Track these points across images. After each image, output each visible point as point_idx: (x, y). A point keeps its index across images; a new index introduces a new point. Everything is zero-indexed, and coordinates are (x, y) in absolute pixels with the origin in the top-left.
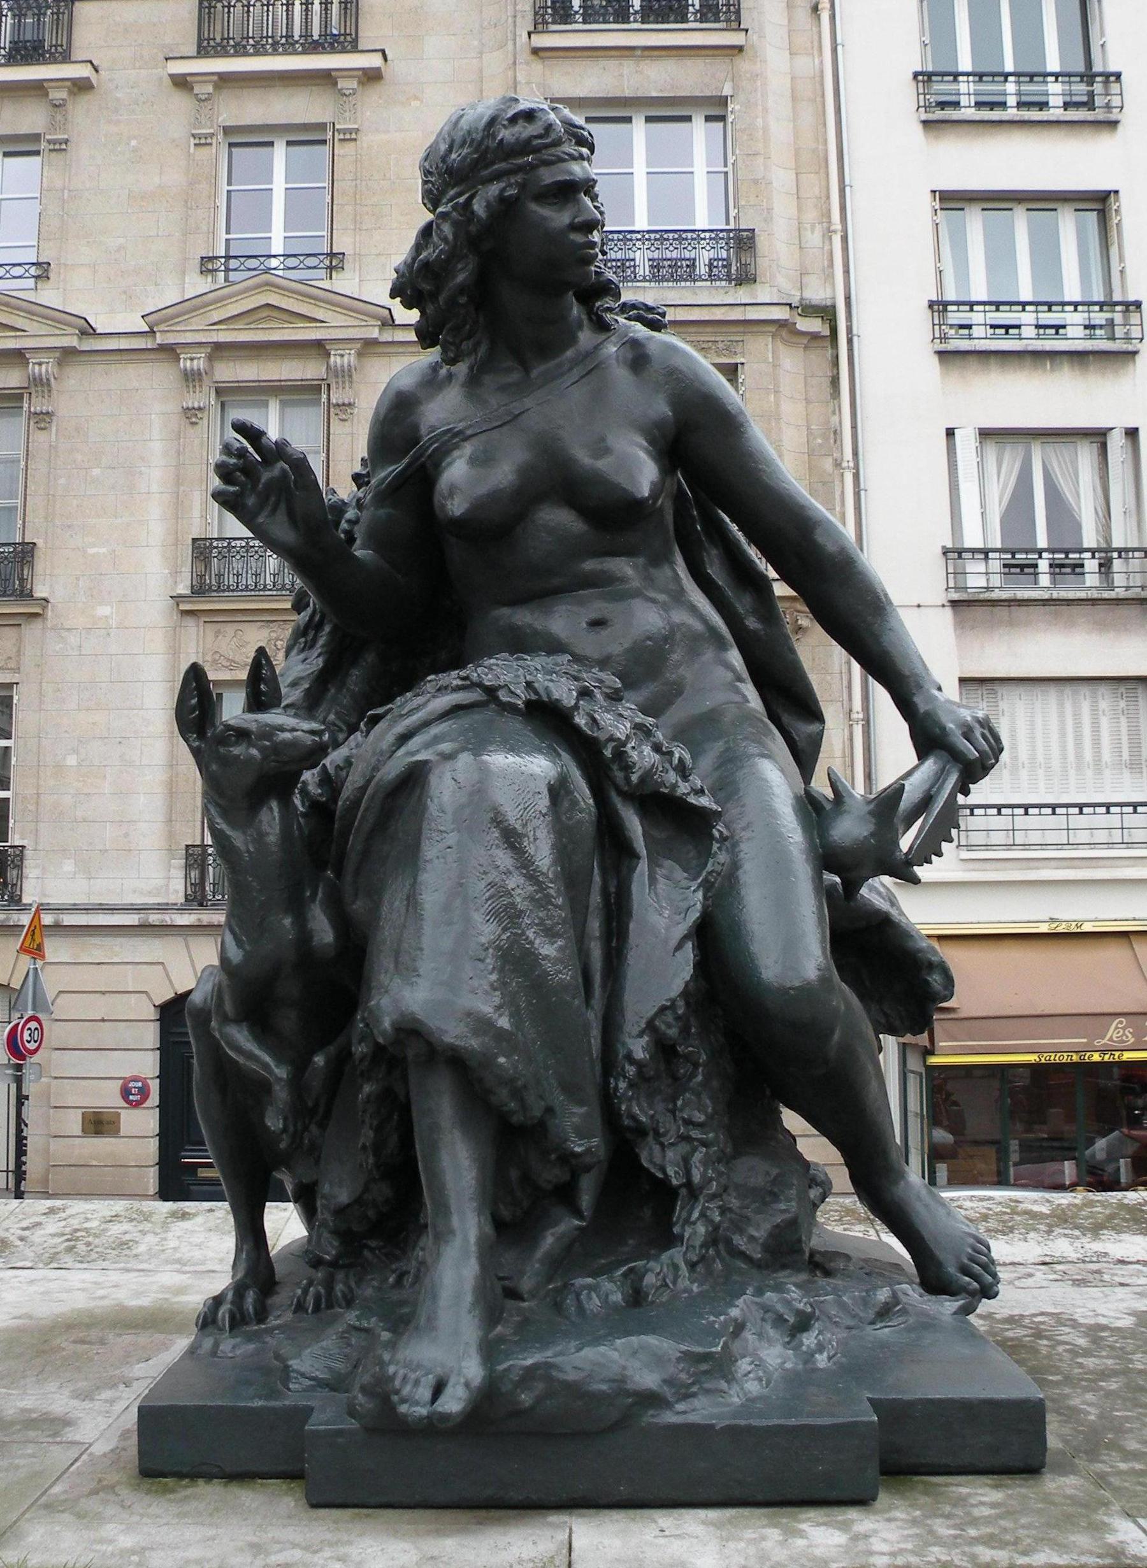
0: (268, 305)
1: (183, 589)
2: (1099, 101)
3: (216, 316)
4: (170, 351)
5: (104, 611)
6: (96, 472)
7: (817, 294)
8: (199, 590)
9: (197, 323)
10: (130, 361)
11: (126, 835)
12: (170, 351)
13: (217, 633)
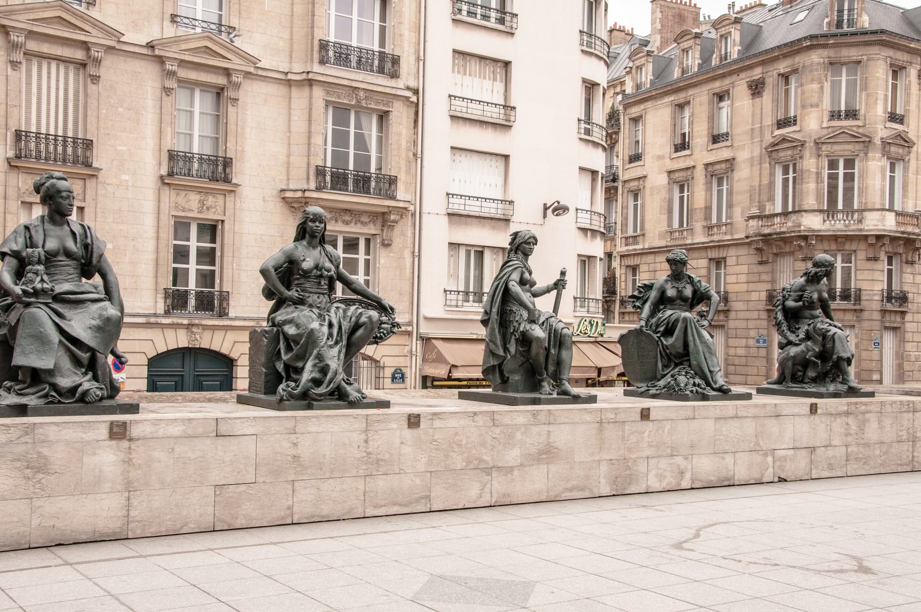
0: (206, 47)
1: (164, 171)
2: (507, 24)
3: (184, 47)
4: (161, 60)
5: (125, 177)
6: (120, 110)
7: (413, 84)
8: (171, 174)
9: (175, 48)
10: (137, 58)
11: (136, 282)
12: (161, 60)
13: (178, 194)
